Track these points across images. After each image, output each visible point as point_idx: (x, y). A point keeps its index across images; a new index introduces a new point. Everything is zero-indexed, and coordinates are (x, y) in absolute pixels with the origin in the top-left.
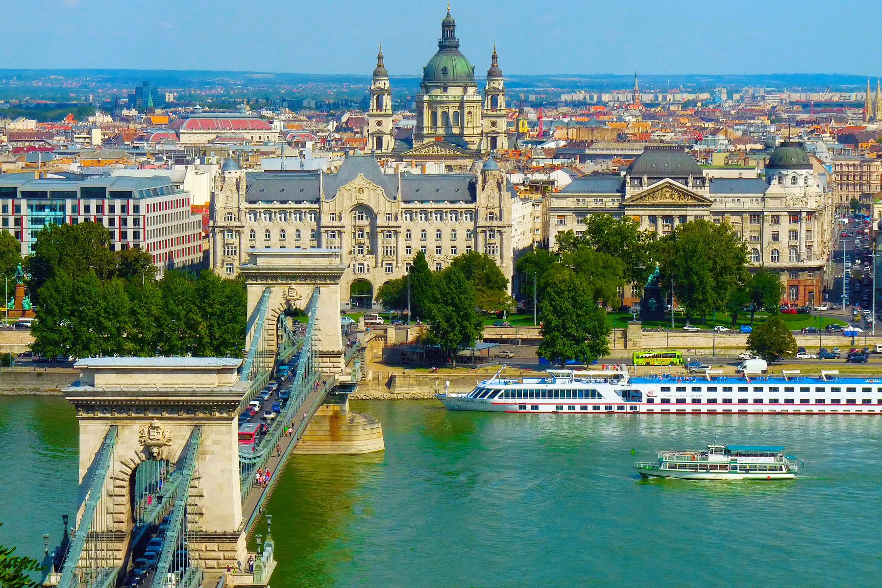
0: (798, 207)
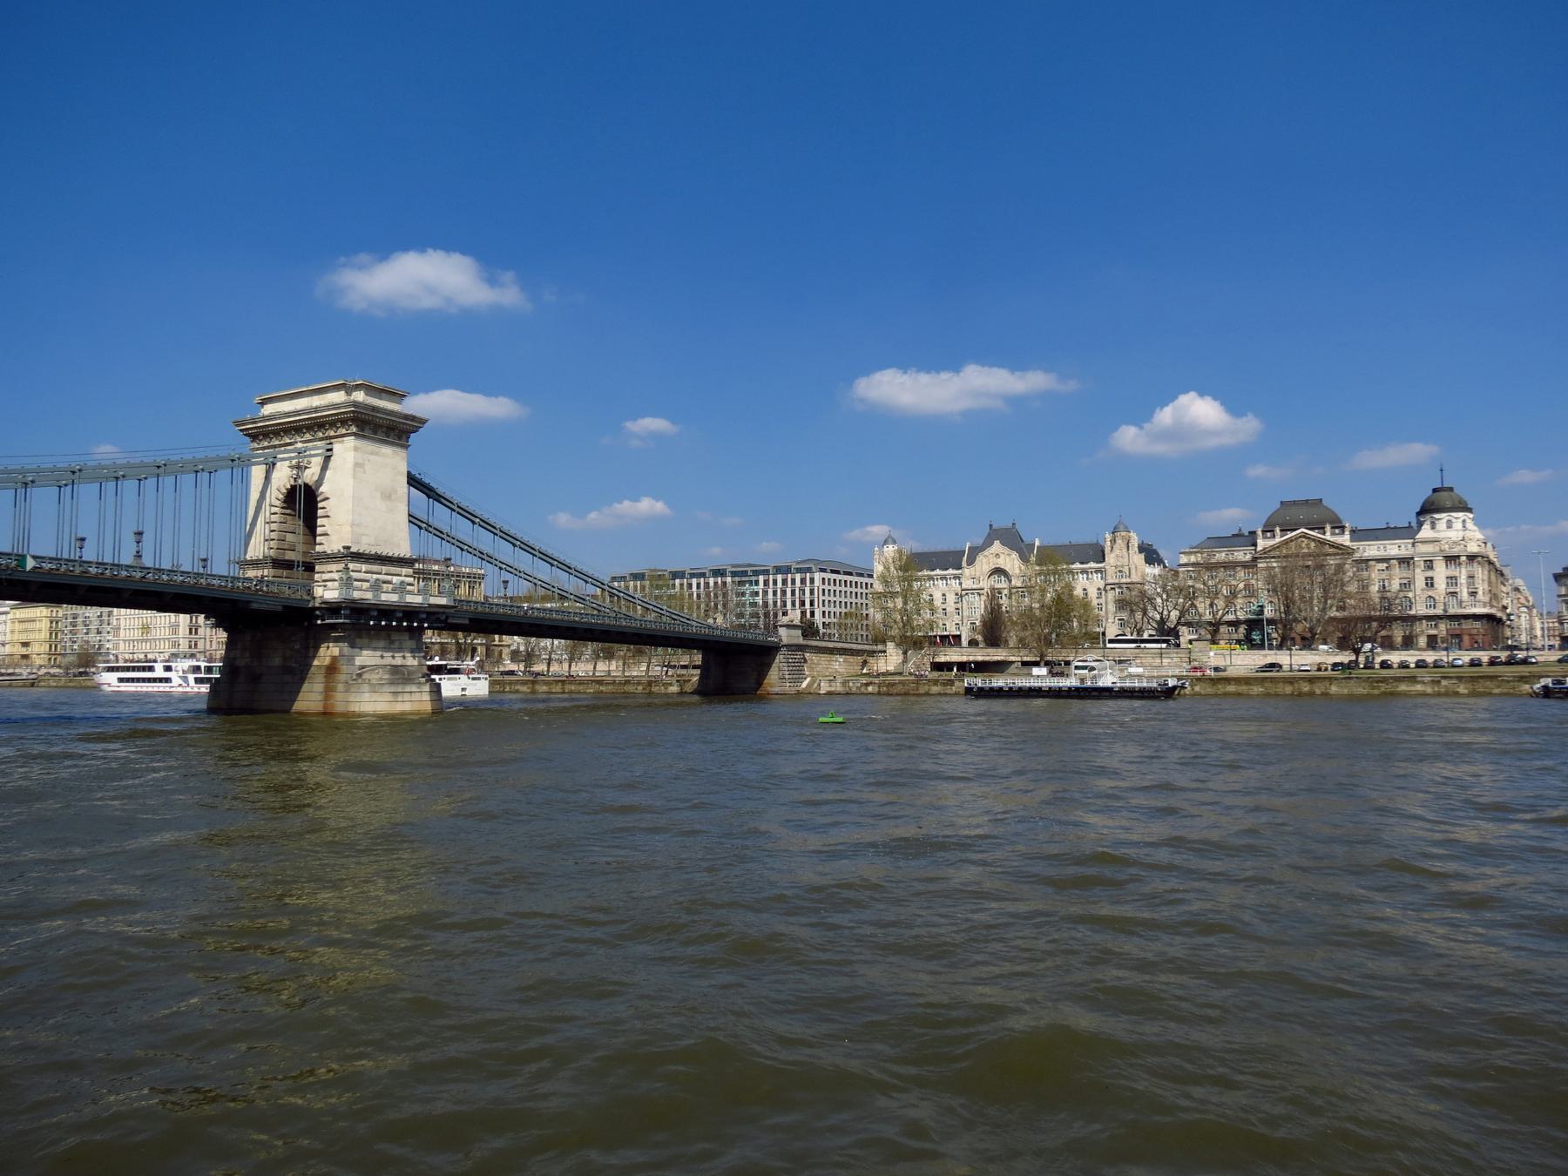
0: (1456, 551)
